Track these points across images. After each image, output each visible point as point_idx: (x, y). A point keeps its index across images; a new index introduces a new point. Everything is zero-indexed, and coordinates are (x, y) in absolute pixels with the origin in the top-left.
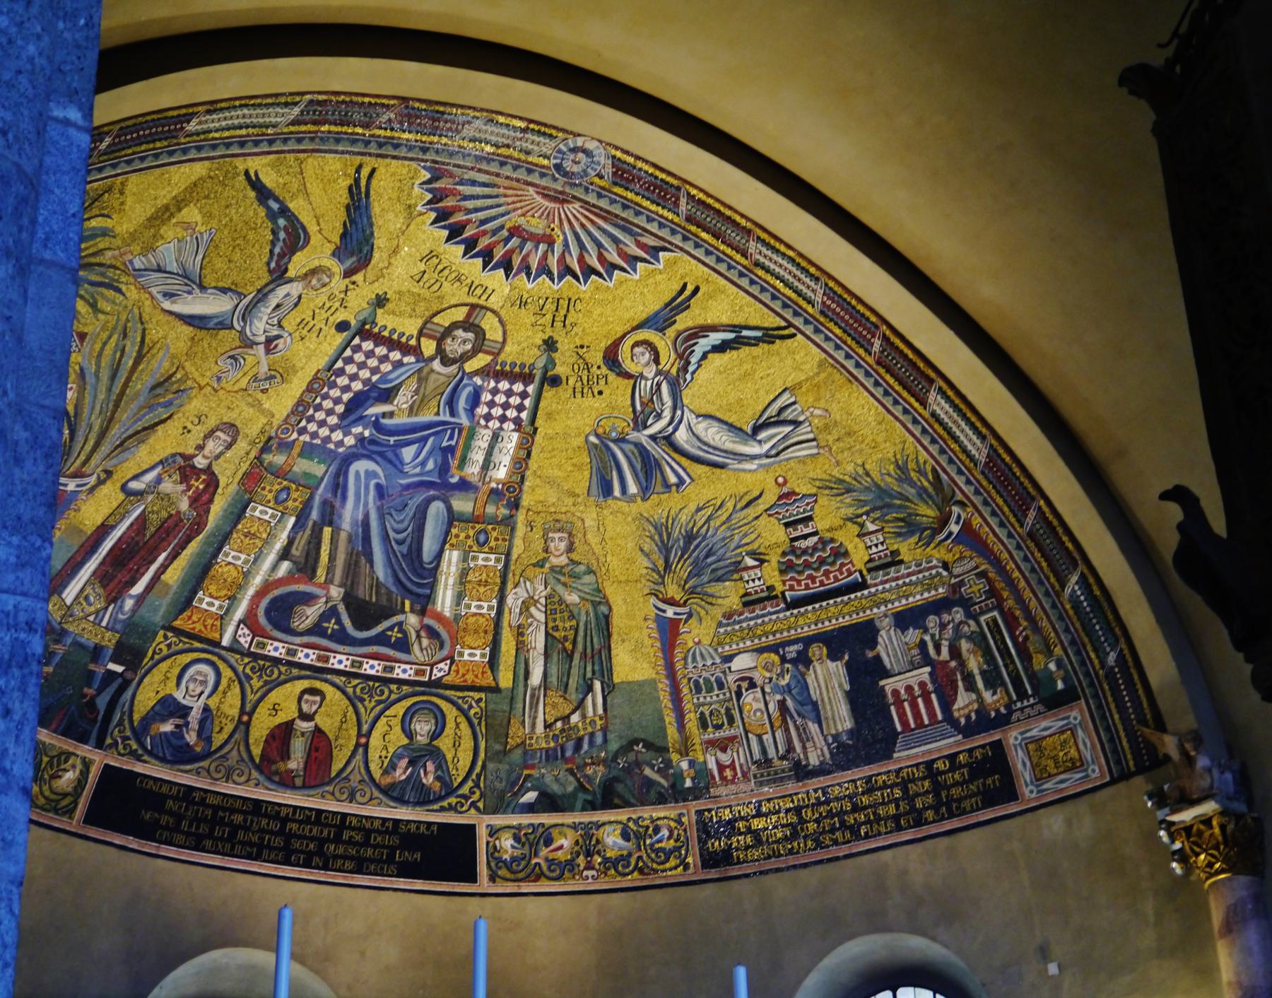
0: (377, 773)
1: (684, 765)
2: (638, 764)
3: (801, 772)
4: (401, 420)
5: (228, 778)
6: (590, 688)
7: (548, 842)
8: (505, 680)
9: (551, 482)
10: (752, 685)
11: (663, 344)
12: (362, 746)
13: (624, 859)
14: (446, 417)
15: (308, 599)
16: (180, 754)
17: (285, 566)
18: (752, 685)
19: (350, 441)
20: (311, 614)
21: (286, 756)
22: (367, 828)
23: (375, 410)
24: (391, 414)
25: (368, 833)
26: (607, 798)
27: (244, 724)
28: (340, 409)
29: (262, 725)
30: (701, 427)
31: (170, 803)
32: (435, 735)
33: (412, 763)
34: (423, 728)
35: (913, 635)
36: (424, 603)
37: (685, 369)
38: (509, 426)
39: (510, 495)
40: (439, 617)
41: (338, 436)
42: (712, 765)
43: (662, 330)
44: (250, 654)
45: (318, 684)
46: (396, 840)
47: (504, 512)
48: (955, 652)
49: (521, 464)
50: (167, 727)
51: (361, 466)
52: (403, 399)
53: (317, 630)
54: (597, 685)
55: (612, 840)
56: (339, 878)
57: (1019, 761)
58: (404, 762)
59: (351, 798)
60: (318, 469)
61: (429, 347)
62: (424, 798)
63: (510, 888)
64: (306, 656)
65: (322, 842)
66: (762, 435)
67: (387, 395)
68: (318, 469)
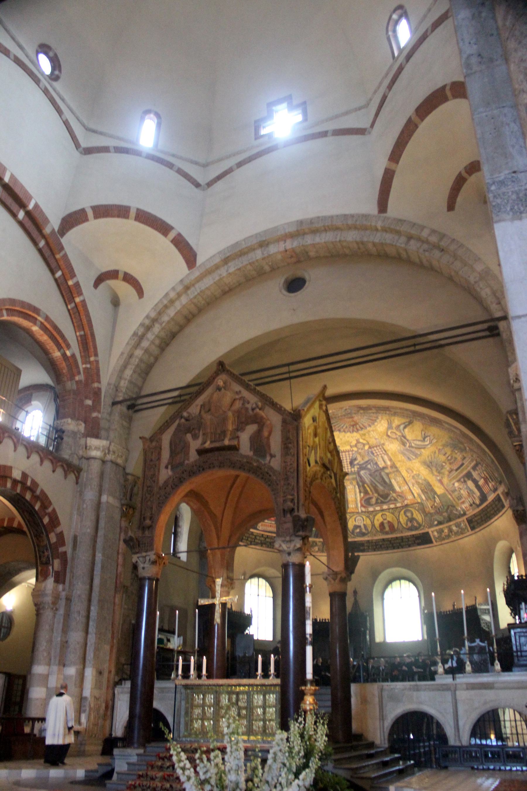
0: (405, 526)
1: (459, 509)
2: (451, 511)
3: (478, 506)
4: (362, 462)
5: (375, 536)
6: (435, 498)
7: (443, 532)
8: (419, 501)
9: (399, 461)
10: (461, 489)
11: (394, 431)
12: (399, 522)
13: (458, 531)
14: (370, 458)
15: (371, 498)
16: (363, 534)
17: (362, 495)
18: (461, 489)
19: (356, 469)
20: (373, 501)
21: (384, 528)
22: (408, 538)
23: (356, 462)
24: (360, 462)
25: (408, 539)
26: (450, 520)
27: (373, 525)
28: (349, 465)
29: (377, 524)
30: (415, 442)
31: (366, 544)
32: (412, 514)
33: (410, 522)
34: (409, 515)
35: (477, 472)
36: (394, 491)
37: (402, 434)
38: (383, 455)
39: (393, 466)
40: (399, 492)
41: (353, 469)
42: (464, 508)
43: (392, 429)
44: (365, 512)
45: (384, 513)
46: (414, 539)
47: (395, 470)
48: (485, 475)
49: (390, 460)
50: (358, 530)
51: (362, 473)
52: (359, 459)
53: (377, 503)
54: (436, 496)
55: (454, 528)
56: (406, 549)
57: (502, 497)
58: (409, 523)
59: (402, 532)
60: (354, 476)
61: (355, 449)
62: (416, 529)
63: (440, 543)
64: (378, 508)
65: (399, 543)
66: (426, 440)
67: (356, 459)
68: (354, 476)
